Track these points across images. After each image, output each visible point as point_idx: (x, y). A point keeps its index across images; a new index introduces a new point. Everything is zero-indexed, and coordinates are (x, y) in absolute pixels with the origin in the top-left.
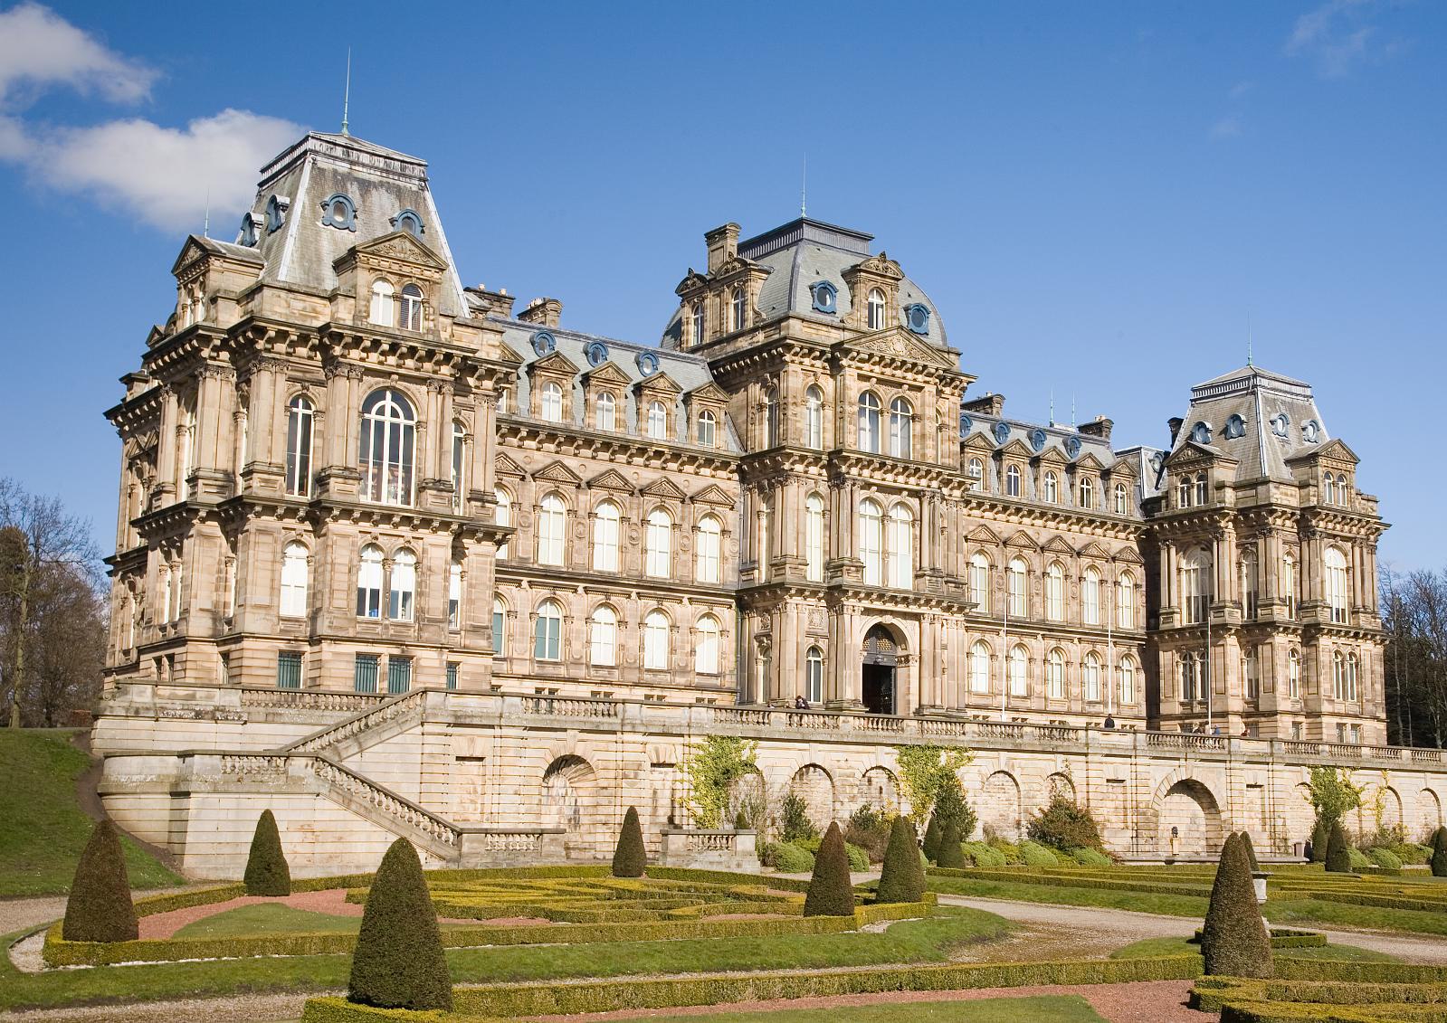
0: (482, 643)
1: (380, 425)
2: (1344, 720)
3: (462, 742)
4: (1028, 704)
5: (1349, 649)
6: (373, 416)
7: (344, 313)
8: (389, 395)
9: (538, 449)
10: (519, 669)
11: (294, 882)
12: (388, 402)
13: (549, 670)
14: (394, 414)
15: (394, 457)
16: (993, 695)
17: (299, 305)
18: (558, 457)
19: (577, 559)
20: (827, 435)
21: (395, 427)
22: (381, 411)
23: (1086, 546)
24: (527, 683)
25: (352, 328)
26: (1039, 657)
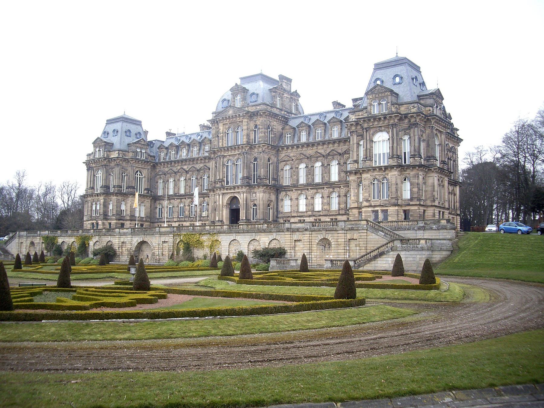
0: (114, 218)
2: (376, 209)
4: (321, 214)
5: (382, 177)
6: (98, 175)
9: (178, 166)
10: (175, 220)
11: (418, 279)
13: (181, 219)
15: (100, 183)
16: (307, 212)
18: (182, 167)
19: (188, 191)
20: (225, 142)
23: (345, 152)
24: (177, 223)
26: (325, 196)
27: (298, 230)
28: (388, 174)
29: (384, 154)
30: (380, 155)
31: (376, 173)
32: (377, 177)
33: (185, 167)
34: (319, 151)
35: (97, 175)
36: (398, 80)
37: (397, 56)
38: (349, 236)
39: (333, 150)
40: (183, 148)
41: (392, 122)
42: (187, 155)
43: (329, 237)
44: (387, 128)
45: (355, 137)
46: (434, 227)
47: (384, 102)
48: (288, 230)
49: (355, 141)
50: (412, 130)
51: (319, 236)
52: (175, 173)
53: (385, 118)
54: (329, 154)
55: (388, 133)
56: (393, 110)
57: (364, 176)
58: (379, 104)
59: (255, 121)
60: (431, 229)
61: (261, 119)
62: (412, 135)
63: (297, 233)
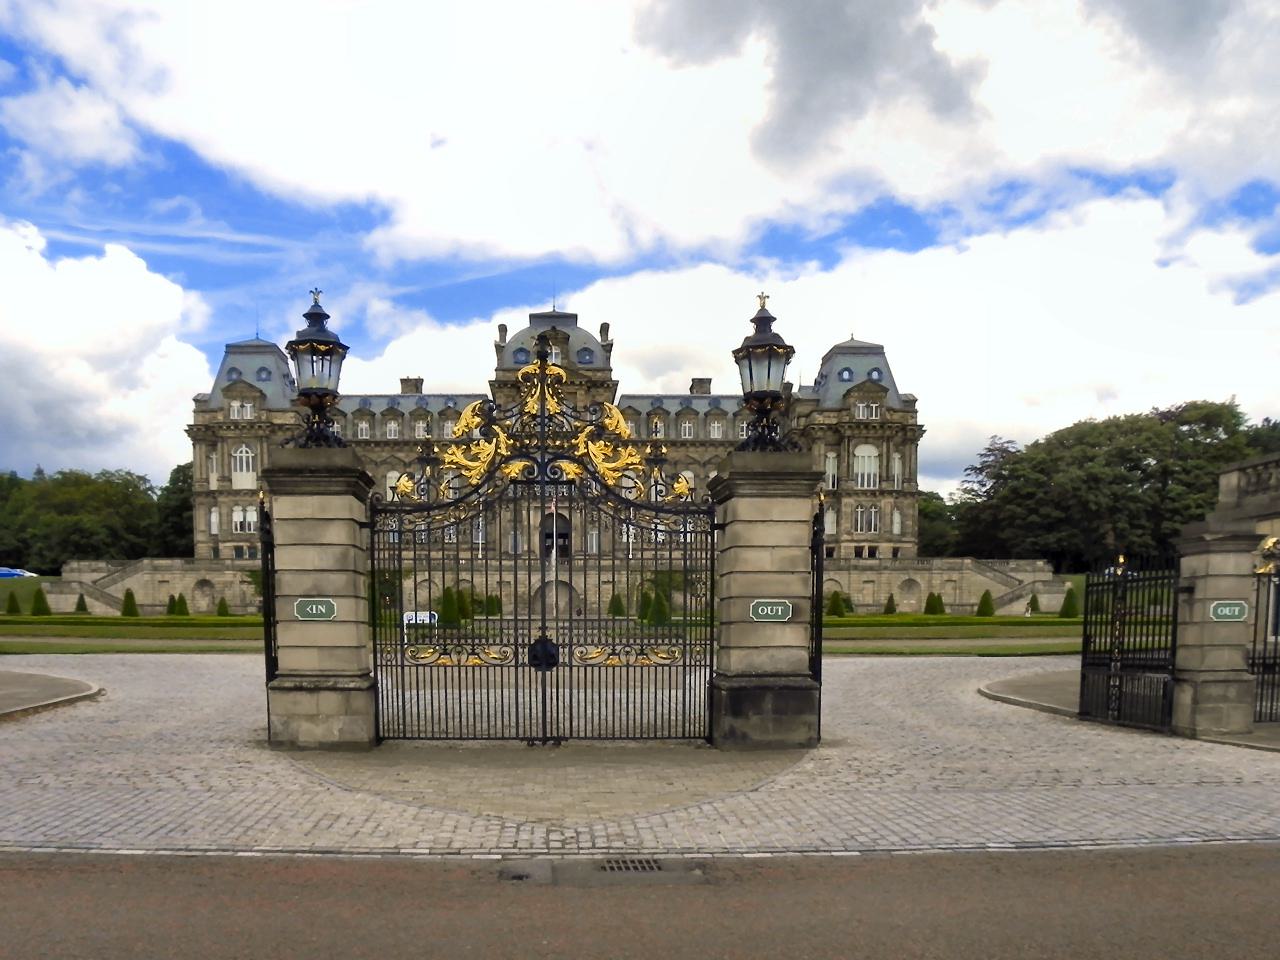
1: (241, 458)
3: (159, 577)
6: (238, 455)
7: (220, 417)
8: (244, 446)
12: (244, 448)
14: (247, 452)
17: (207, 416)
21: (248, 457)
22: (241, 452)
25: (224, 423)
27: (871, 568)
28: (880, 501)
29: (869, 476)
30: (863, 476)
31: (862, 499)
32: (864, 503)
33: (401, 455)
34: (691, 455)
35: (235, 452)
36: (846, 375)
37: (852, 339)
38: (946, 577)
39: (717, 456)
40: (390, 419)
41: (888, 433)
42: (401, 433)
43: (918, 578)
44: (876, 441)
45: (823, 446)
46: (1028, 568)
47: (874, 406)
48: (856, 568)
49: (822, 452)
50: (907, 447)
51: (902, 576)
52: (376, 464)
53: (882, 427)
54: (709, 462)
55: (878, 447)
56: (888, 417)
57: (845, 500)
58: (868, 406)
59: (594, 396)
60: (1026, 571)
61: (606, 394)
62: (907, 453)
63: (869, 572)
